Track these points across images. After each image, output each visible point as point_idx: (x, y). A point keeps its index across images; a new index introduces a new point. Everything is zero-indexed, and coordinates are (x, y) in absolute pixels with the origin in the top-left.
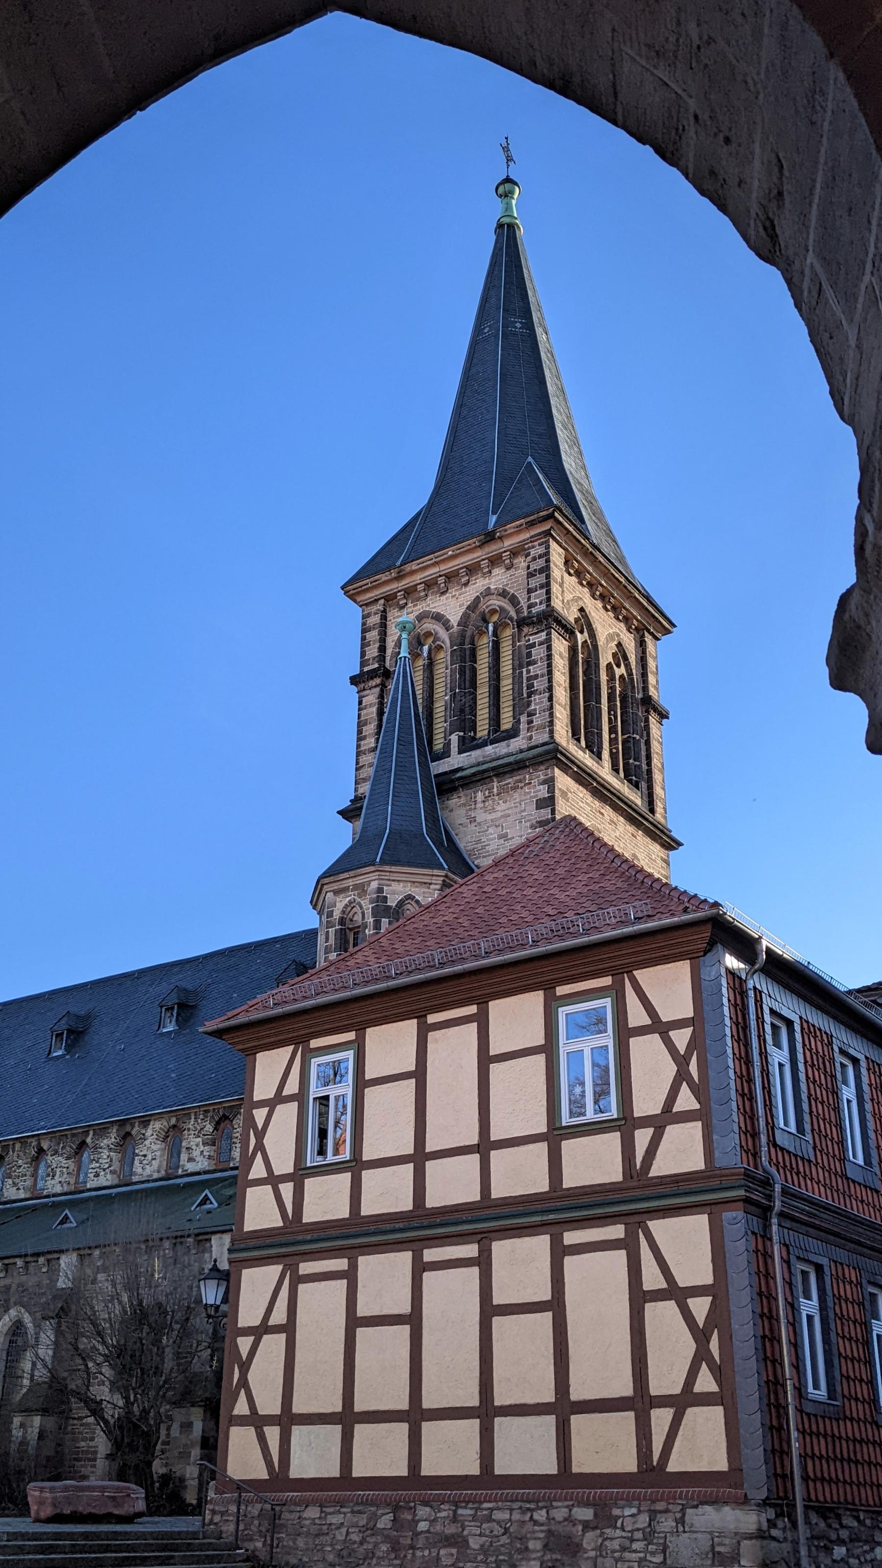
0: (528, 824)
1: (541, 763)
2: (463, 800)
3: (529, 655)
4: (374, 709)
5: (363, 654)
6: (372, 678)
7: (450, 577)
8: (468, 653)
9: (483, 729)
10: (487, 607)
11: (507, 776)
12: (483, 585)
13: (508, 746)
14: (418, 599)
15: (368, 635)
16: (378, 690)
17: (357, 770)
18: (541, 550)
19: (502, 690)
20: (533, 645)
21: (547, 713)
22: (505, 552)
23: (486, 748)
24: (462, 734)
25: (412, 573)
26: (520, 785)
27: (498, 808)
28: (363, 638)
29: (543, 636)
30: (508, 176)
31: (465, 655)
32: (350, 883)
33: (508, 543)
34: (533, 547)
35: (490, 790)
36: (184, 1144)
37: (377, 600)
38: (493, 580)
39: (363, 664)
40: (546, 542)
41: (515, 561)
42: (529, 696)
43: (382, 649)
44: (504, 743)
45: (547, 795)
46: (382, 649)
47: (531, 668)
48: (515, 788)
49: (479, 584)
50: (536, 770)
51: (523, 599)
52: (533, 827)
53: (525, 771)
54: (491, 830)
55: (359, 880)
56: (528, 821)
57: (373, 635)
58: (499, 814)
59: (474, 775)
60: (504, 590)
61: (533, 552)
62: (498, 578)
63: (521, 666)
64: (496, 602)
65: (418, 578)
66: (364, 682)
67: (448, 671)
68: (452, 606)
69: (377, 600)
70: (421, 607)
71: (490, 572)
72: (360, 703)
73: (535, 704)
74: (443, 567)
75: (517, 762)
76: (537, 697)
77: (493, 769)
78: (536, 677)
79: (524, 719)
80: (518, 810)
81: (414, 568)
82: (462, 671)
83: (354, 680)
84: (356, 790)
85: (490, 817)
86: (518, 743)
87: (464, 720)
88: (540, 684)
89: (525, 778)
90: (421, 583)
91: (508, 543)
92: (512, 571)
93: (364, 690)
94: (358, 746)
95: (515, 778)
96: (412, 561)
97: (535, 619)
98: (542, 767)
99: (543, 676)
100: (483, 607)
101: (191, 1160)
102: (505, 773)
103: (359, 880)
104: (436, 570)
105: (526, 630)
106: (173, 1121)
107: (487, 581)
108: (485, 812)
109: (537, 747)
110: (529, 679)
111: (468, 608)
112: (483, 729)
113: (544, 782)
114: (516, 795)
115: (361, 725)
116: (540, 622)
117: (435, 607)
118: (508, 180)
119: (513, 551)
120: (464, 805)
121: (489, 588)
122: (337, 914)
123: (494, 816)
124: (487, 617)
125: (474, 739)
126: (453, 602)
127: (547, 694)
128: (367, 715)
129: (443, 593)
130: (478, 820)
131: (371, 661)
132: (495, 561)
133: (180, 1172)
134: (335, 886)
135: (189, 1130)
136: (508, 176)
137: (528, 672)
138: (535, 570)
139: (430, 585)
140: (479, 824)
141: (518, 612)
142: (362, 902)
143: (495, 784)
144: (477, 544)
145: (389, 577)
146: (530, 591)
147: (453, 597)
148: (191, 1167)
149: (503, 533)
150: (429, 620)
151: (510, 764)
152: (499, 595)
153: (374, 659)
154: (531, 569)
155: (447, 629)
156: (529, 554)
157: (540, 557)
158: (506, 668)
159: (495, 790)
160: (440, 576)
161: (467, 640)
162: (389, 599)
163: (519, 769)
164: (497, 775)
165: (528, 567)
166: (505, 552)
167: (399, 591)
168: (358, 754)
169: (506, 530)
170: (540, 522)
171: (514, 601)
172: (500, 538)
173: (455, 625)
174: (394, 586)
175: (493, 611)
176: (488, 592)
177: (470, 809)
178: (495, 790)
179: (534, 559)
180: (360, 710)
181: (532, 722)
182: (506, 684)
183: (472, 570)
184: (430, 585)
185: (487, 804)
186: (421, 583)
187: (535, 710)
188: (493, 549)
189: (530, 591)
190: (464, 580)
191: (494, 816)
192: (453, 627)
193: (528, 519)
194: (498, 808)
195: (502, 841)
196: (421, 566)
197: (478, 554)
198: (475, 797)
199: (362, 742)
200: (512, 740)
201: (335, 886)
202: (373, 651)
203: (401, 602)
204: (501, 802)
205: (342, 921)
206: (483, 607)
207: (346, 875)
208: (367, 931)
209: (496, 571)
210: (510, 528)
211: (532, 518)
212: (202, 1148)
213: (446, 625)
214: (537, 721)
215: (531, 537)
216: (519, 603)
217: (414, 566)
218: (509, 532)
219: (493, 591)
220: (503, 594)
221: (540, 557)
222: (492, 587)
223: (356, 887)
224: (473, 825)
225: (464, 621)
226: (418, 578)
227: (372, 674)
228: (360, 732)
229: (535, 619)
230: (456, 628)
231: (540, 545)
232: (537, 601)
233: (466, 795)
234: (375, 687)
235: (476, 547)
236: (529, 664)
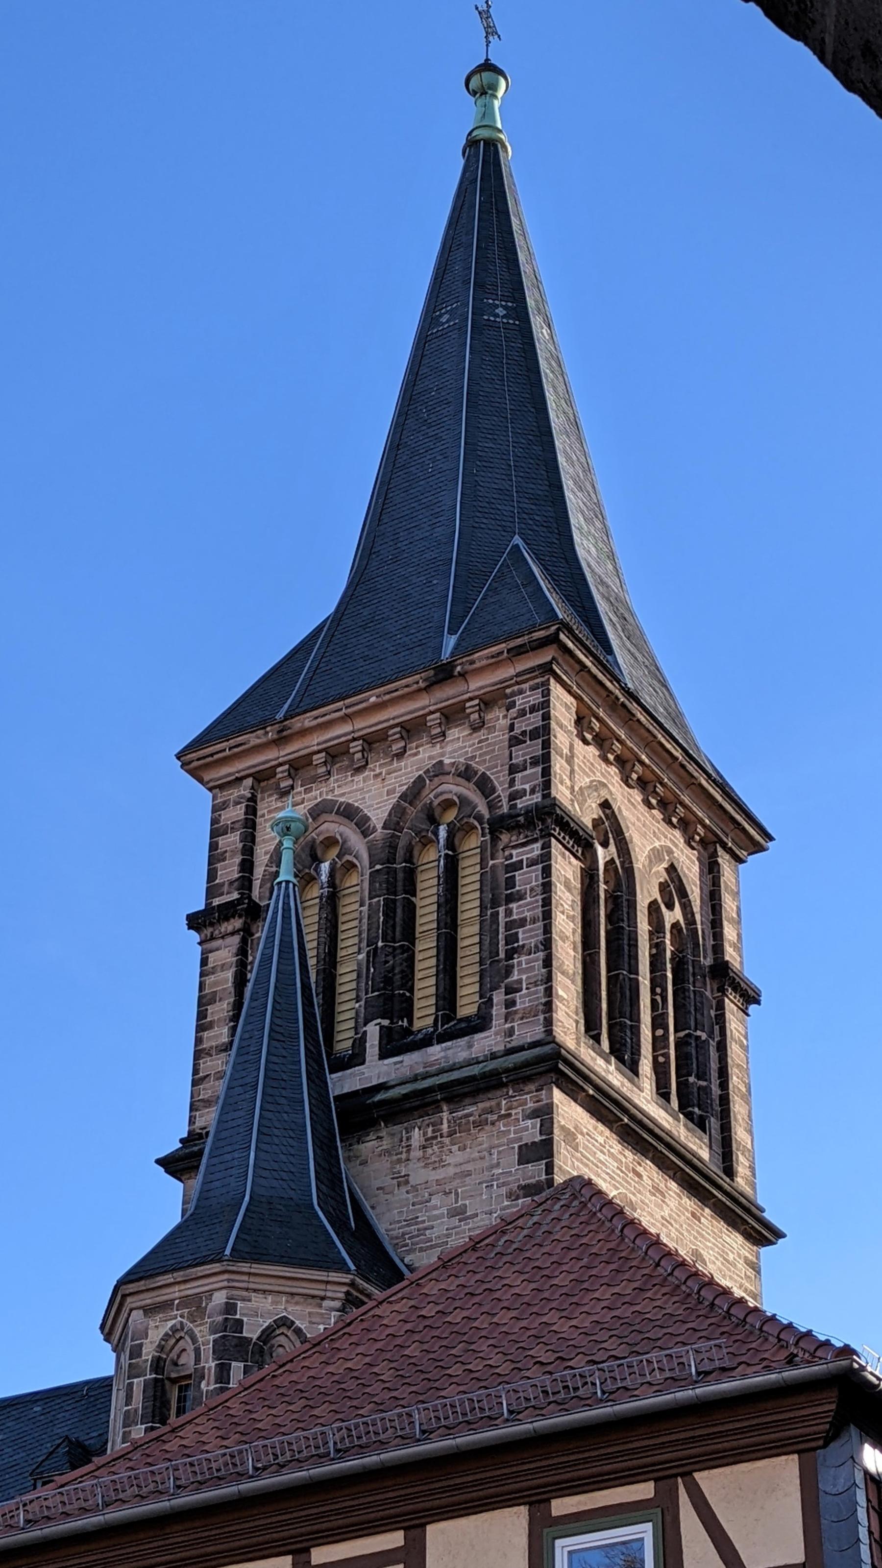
0: (504, 1190)
1: (528, 1079)
2: (386, 1144)
3: (510, 883)
4: (229, 975)
5: (212, 875)
6: (227, 919)
7: (373, 742)
8: (400, 876)
9: (424, 1013)
10: (436, 797)
11: (467, 1101)
12: (430, 758)
13: (470, 1046)
14: (314, 779)
15: (222, 841)
16: (236, 939)
17: (195, 1083)
18: (535, 698)
19: (461, 944)
20: (518, 866)
21: (541, 988)
22: (471, 699)
23: (431, 1050)
24: (386, 1022)
25: (304, 732)
26: (492, 1117)
27: (449, 1159)
28: (213, 847)
29: (536, 849)
30: (487, 60)
31: (396, 880)
32: (175, 1293)
33: (477, 684)
34: (521, 692)
35: (437, 1124)
37: (240, 780)
38: (449, 749)
39: (211, 892)
40: (543, 684)
41: (489, 716)
42: (510, 955)
43: (247, 866)
44: (462, 1042)
45: (538, 1138)
46: (247, 866)
47: (514, 906)
48: (480, 1124)
49: (423, 755)
50: (521, 1092)
51: (501, 784)
52: (509, 1195)
53: (499, 1093)
54: (435, 1201)
55: (191, 1289)
56: (504, 1184)
57: (232, 841)
58: (451, 1171)
59: (406, 1097)
60: (468, 767)
61: (519, 701)
62: (458, 746)
63: (495, 903)
64: (453, 788)
65: (314, 742)
66: (212, 924)
67: (365, 909)
68: (375, 793)
69: (240, 780)
70: (318, 794)
71: (443, 734)
72: (204, 962)
73: (521, 972)
75: (484, 1076)
76: (523, 958)
77: (442, 1087)
78: (522, 922)
79: (499, 997)
80: (485, 1164)
81: (308, 724)
82: (390, 908)
83: (195, 922)
84: (192, 1121)
85: (434, 1175)
86: (486, 1042)
87: (390, 996)
88: (527, 936)
89: (499, 1105)
90: (319, 752)
91: (477, 684)
92: (482, 734)
93: (212, 938)
94: (198, 1041)
95: (481, 1105)
96: (305, 712)
97: (521, 819)
98: (532, 1087)
99: (534, 921)
100: (429, 796)
102: (465, 1095)
103: (191, 1289)
104: (347, 728)
105: (505, 838)
108: (426, 1166)
109: (521, 1049)
110: (509, 926)
112: (424, 1013)
113: (534, 1114)
114: (483, 1137)
115: (204, 1002)
116: (530, 824)
117: (343, 794)
118: (487, 66)
119: (487, 698)
120: (388, 1152)
121: (441, 763)
122: (149, 1352)
123: (440, 1174)
124: (437, 814)
125: (408, 1032)
126: (375, 786)
127: (541, 955)
128: (216, 984)
129: (359, 770)
130: (413, 1181)
131: (226, 888)
132: (452, 715)
134: (148, 1299)
136: (487, 60)
137: (508, 913)
138: (524, 733)
139: (335, 755)
140: (415, 1188)
141: (491, 806)
142: (196, 1331)
143: (445, 1115)
144: (422, 685)
145: (264, 740)
146: (513, 769)
147: (376, 776)
149: (468, 667)
150: (333, 817)
151: (472, 1078)
152: (459, 775)
153: (231, 883)
154: (517, 731)
155: (365, 834)
156: (512, 705)
157: (533, 709)
158: (469, 905)
159: (445, 1126)
160: (354, 739)
161: (400, 853)
162: (262, 777)
163: (488, 1089)
164: (449, 1100)
165: (512, 728)
166: (471, 699)
167: (281, 765)
168: (198, 1055)
169: (472, 662)
170: (533, 649)
171: (485, 786)
172: (462, 675)
173: (379, 826)
174: (271, 755)
175: (448, 804)
176: (438, 770)
177: (399, 1161)
178: (445, 1126)
179: (522, 713)
180: (202, 974)
181: (513, 1003)
182: (469, 934)
183: (412, 730)
184: (335, 755)
185: (429, 1151)
186: (319, 752)
187: (520, 981)
188: (448, 693)
189: (513, 769)
190: (397, 747)
191: (440, 1174)
192: (374, 830)
193: (512, 644)
194: (449, 1159)
195: (455, 1221)
196: (320, 720)
197: (423, 702)
198: (408, 1139)
199: (206, 1034)
200: (477, 1036)
201: (148, 1299)
202: (230, 870)
203: (282, 785)
204: (455, 1148)
205: (158, 1365)
206: (429, 796)
207: (168, 1278)
208: (203, 1385)
209: (454, 733)
210: (480, 659)
211: (519, 641)
213: (363, 825)
214: (523, 1001)
215: (517, 675)
216: (493, 790)
217: (307, 721)
218: (478, 665)
219: (447, 769)
220: (466, 773)
221: (533, 709)
222: (447, 761)
223: (185, 1301)
224: (404, 1189)
225: (395, 821)
226: (314, 742)
227: (227, 911)
228: (202, 1015)
229: (521, 819)
230: (380, 833)
231: (532, 689)
232: (527, 787)
233: (393, 1135)
234: (232, 934)
235: (420, 690)
236: (510, 899)
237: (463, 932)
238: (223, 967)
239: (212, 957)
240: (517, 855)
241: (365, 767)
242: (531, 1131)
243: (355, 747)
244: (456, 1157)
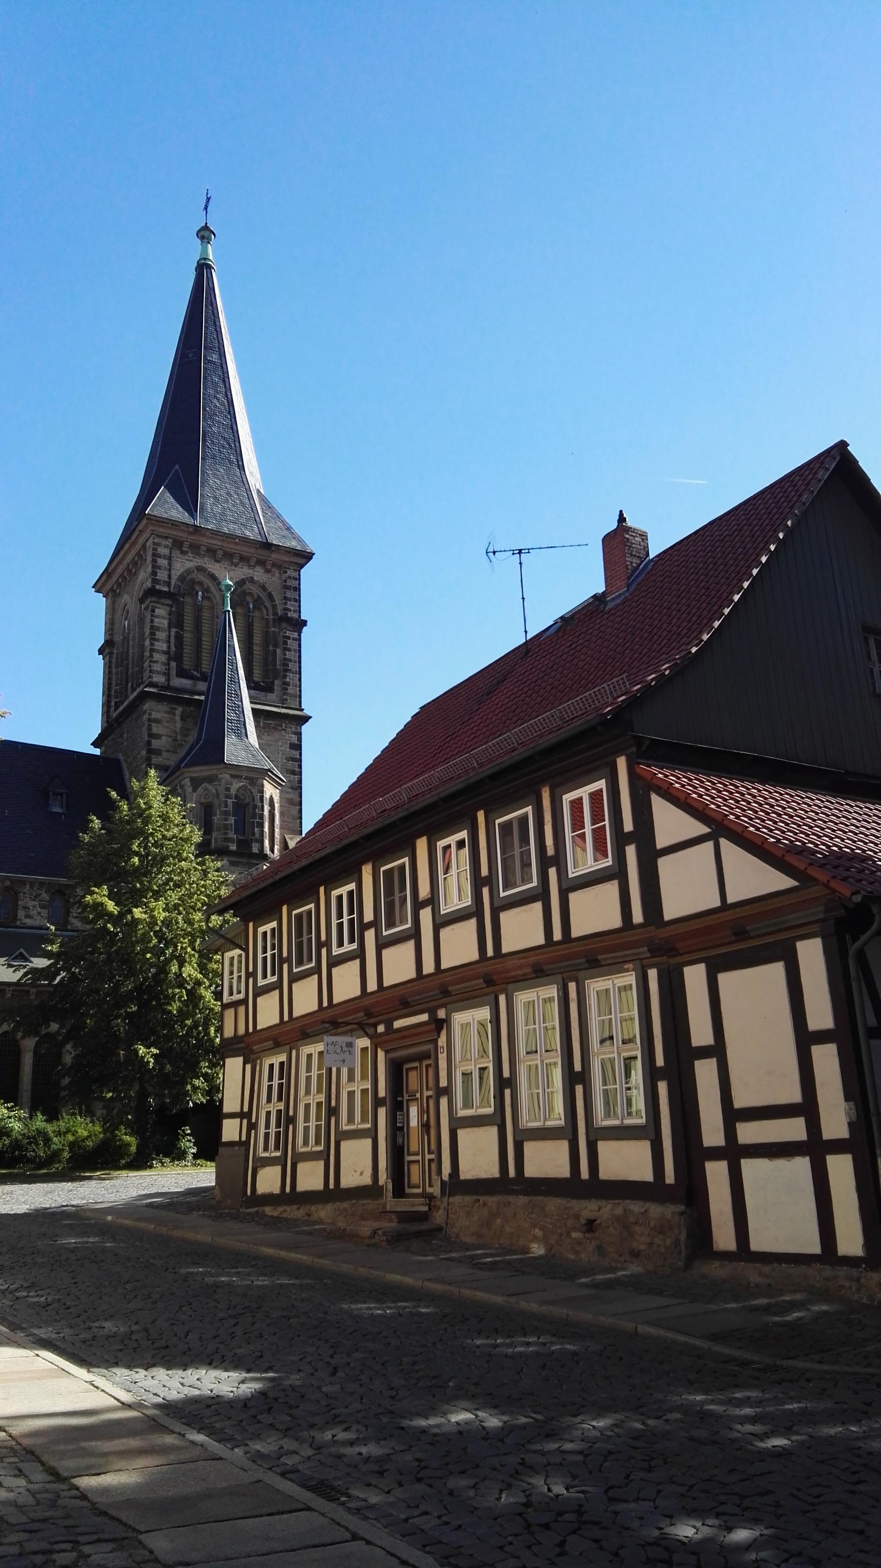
14: (198, 554)
26: (279, 728)
36: (20, 903)
37: (166, 538)
42: (286, 670)
46: (170, 576)
52: (286, 759)
62: (259, 574)
63: (276, 645)
64: (255, 590)
71: (254, 566)
92: (269, 575)
100: (245, 587)
101: (27, 916)
106: (8, 883)
107: (251, 571)
113: (295, 733)
132: (261, 563)
133: (18, 923)
135: (24, 893)
148: (29, 922)
156: (286, 572)
203: (184, 549)
206: (248, 586)
209: (258, 568)
212: (39, 910)
216: (274, 601)
237: (255, 648)
240: (288, 633)
241: (219, 562)
243: (220, 553)
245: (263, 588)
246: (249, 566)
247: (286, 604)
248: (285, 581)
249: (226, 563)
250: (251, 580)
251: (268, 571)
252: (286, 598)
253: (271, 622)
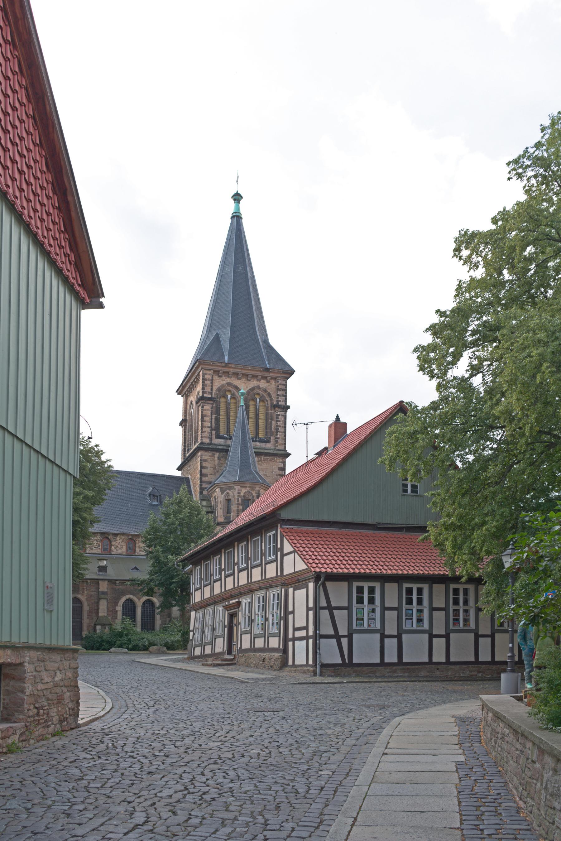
14: (228, 377)
37: (210, 370)
42: (277, 432)
44: (264, 444)
48: (270, 461)
49: (254, 383)
62: (263, 384)
63: (272, 419)
74: (243, 371)
78: (280, 426)
86: (268, 445)
92: (269, 384)
100: (255, 391)
107: (258, 383)
111: (250, 389)
113: (282, 462)
114: (271, 463)
122: (242, 494)
179: (281, 384)
182: (262, 422)
205: (244, 496)
209: (262, 381)
226: (231, 370)
238: (208, 410)
239: (205, 407)
240: (279, 413)
241: (240, 379)
242: (281, 465)
243: (240, 375)
244: (265, 465)
245: (265, 391)
246: (257, 380)
247: (278, 398)
248: (278, 386)
249: (244, 380)
250: (258, 387)
251: (268, 382)
252: (278, 395)
253: (269, 407)
